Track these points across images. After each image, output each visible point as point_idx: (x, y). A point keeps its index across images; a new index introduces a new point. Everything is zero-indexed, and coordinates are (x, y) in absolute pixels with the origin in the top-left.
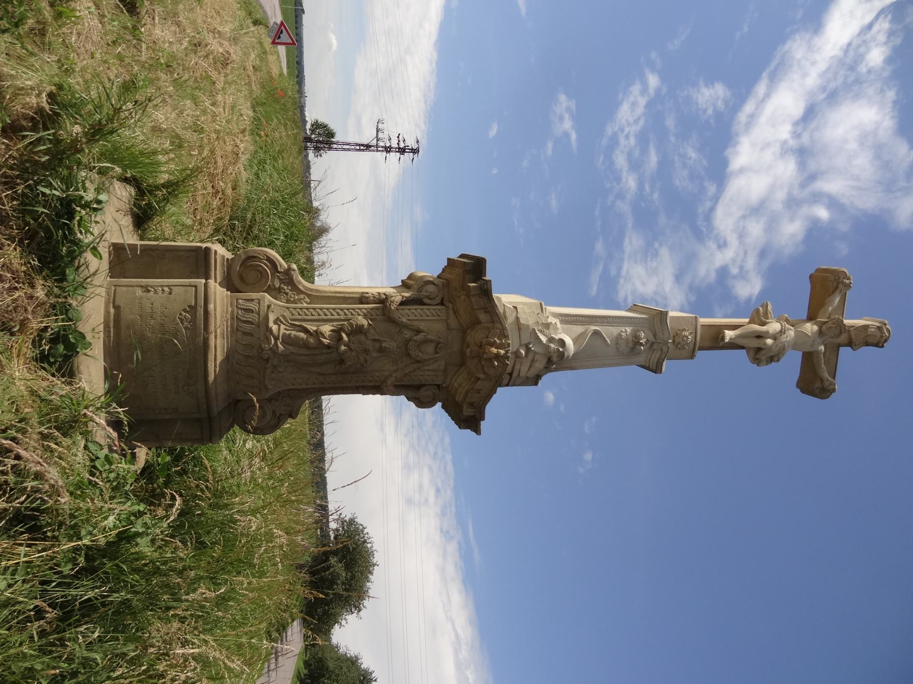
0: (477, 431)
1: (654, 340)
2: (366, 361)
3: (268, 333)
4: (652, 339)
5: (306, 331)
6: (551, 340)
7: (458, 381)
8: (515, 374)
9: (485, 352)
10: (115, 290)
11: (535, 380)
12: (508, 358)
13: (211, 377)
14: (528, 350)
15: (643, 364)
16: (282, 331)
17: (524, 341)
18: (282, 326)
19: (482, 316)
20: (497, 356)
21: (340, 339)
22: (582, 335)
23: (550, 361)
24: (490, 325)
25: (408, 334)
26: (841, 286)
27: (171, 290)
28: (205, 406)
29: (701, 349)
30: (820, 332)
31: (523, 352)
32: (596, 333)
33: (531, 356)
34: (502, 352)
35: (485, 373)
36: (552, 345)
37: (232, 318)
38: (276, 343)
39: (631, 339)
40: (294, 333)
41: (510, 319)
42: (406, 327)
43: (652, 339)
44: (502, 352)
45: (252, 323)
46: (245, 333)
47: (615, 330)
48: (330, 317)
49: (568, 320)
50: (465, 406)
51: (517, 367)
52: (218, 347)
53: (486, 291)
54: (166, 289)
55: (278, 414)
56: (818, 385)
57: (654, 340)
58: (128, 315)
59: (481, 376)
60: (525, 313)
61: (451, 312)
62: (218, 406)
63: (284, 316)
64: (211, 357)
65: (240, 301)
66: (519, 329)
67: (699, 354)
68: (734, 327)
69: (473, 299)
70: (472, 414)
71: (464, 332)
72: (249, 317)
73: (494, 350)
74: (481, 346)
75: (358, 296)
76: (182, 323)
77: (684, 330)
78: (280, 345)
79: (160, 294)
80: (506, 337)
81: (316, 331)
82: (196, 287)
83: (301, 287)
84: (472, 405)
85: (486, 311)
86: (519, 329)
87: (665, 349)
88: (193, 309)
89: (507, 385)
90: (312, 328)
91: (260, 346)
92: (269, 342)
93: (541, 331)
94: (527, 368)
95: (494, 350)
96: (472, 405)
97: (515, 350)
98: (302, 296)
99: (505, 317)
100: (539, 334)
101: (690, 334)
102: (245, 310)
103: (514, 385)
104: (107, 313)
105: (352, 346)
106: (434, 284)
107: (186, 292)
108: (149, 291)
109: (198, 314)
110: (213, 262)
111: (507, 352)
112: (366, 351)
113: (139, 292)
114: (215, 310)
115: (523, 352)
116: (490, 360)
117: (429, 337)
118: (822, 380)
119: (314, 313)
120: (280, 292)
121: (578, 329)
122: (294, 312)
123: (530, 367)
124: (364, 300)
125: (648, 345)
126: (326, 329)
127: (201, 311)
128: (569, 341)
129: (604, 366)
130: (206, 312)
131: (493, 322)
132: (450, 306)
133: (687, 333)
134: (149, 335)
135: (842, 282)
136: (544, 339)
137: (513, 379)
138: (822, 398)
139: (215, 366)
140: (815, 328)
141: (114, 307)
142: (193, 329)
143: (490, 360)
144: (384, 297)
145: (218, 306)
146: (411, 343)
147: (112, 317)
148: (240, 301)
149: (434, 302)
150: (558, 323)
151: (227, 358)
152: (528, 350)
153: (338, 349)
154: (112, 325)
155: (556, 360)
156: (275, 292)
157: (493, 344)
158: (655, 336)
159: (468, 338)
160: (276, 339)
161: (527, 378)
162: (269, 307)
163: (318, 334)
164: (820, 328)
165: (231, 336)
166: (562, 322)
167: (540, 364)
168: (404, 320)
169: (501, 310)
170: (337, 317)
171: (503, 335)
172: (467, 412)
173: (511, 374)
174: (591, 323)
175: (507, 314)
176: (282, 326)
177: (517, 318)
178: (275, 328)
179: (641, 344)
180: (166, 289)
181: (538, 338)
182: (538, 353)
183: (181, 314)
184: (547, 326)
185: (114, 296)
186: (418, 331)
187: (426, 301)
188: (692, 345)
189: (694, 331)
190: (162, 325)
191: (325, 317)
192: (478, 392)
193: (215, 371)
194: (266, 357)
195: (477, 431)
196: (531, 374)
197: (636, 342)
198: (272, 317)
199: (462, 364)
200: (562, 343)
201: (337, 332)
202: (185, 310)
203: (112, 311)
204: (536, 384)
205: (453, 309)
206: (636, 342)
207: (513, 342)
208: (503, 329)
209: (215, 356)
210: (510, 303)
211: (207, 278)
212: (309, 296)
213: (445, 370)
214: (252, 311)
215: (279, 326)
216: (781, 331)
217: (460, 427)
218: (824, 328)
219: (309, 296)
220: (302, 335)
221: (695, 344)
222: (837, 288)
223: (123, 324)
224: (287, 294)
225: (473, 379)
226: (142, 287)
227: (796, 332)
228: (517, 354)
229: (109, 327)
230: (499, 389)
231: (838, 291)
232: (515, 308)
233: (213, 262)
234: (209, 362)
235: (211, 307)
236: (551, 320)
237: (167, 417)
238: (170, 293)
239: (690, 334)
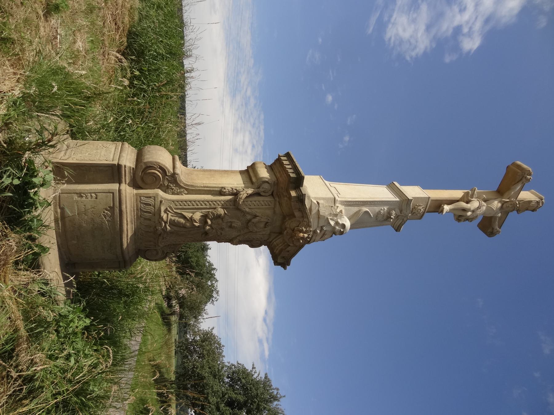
0: (285, 268)
2: (221, 234)
3: (160, 220)
4: (399, 213)
5: (184, 217)
6: (337, 223)
13: (125, 245)
16: (170, 217)
17: (320, 225)
18: (170, 214)
19: (297, 214)
21: (206, 222)
22: (357, 213)
25: (249, 217)
26: (524, 180)
27: (96, 195)
29: (428, 212)
30: (502, 207)
32: (366, 212)
34: (306, 235)
35: (293, 244)
36: (337, 228)
37: (137, 209)
38: (165, 226)
40: (177, 219)
41: (314, 211)
42: (248, 213)
43: (399, 213)
45: (150, 213)
46: (145, 219)
47: (377, 209)
48: (200, 206)
52: (129, 229)
54: (93, 195)
55: (165, 252)
56: (490, 230)
59: (291, 245)
61: (277, 203)
63: (170, 208)
64: (125, 236)
65: (142, 198)
66: (319, 218)
68: (450, 202)
69: (292, 203)
72: (148, 208)
75: (219, 189)
77: (420, 206)
78: (168, 227)
81: (191, 218)
82: (113, 193)
83: (182, 185)
85: (300, 210)
86: (319, 218)
88: (112, 209)
90: (188, 215)
91: (155, 227)
92: (161, 225)
98: (182, 190)
102: (145, 204)
105: (214, 226)
106: (269, 183)
107: (107, 197)
108: (82, 197)
109: (115, 209)
110: (124, 177)
112: (222, 229)
113: (76, 197)
114: (126, 208)
115: (318, 231)
117: (262, 220)
118: (493, 229)
119: (190, 204)
120: (168, 188)
122: (177, 203)
124: (222, 193)
126: (197, 216)
127: (117, 210)
129: (366, 227)
130: (121, 211)
131: (303, 217)
132: (277, 199)
133: (420, 208)
134: (84, 225)
135: (526, 177)
136: (332, 223)
138: (489, 237)
139: (127, 240)
140: (500, 205)
141: (60, 208)
144: (235, 191)
146: (250, 223)
148: (142, 198)
149: (267, 194)
151: (135, 234)
152: (322, 229)
153: (204, 228)
156: (166, 189)
157: (301, 231)
159: (286, 223)
160: (166, 223)
162: (161, 202)
163: (192, 220)
164: (503, 205)
165: (137, 220)
168: (247, 210)
170: (205, 206)
171: (308, 225)
176: (170, 214)
178: (164, 216)
180: (93, 195)
181: (329, 223)
183: (104, 212)
186: (256, 216)
187: (261, 194)
190: (93, 219)
191: (196, 207)
192: (288, 252)
193: (127, 242)
194: (159, 233)
197: (389, 217)
198: (163, 209)
200: (344, 226)
201: (205, 217)
202: (107, 210)
203: (59, 211)
205: (279, 202)
209: (127, 234)
210: (315, 198)
212: (186, 189)
213: (270, 234)
214: (150, 205)
215: (168, 214)
216: (478, 208)
218: (505, 206)
219: (186, 189)
220: (182, 221)
222: (521, 180)
224: (172, 189)
226: (77, 193)
227: (487, 207)
231: (521, 182)
232: (318, 203)
233: (124, 173)
235: (124, 207)
238: (96, 198)
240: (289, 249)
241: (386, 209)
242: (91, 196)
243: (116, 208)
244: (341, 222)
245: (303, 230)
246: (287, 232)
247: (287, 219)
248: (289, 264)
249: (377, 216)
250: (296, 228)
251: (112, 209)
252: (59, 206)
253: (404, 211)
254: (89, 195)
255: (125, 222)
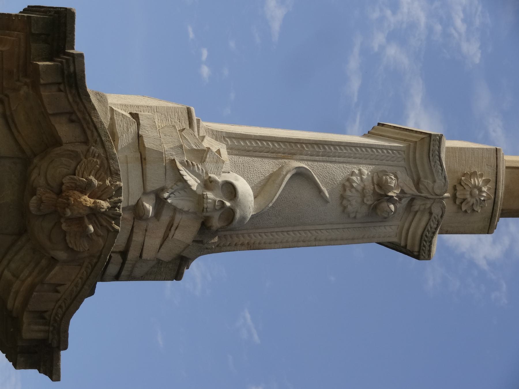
0: (52, 371)
1: (415, 191)
4: (411, 190)
6: (208, 184)
7: (13, 265)
8: (132, 254)
9: (68, 205)
11: (174, 268)
12: (116, 218)
14: (160, 203)
15: (395, 240)
17: (153, 185)
19: (64, 130)
20: (94, 213)
22: (272, 178)
23: (205, 226)
24: (81, 149)
29: (508, 213)
31: (149, 207)
32: (301, 175)
33: (165, 218)
34: (105, 204)
35: (68, 249)
36: (210, 195)
39: (370, 188)
43: (411, 190)
44: (105, 204)
49: (245, 147)
50: (26, 319)
51: (137, 238)
53: (72, 76)
57: (415, 191)
59: (62, 255)
60: (154, 126)
66: (143, 160)
67: (502, 223)
69: (45, 93)
70: (40, 335)
71: (25, 162)
73: (88, 201)
74: (60, 193)
77: (474, 174)
80: (115, 174)
84: (40, 316)
86: (143, 160)
87: (436, 210)
89: (117, 278)
93: (187, 165)
94: (158, 242)
95: (88, 201)
96: (40, 316)
97: (132, 202)
99: (114, 134)
100: (183, 172)
101: (487, 182)
103: (131, 278)
111: (115, 205)
115: (149, 207)
116: (79, 221)
121: (266, 166)
123: (165, 238)
125: (405, 201)
128: (244, 186)
129: (317, 242)
131: (86, 142)
133: (479, 181)
136: (193, 182)
137: (128, 266)
143: (79, 221)
150: (224, 152)
152: (160, 203)
155: (217, 228)
157: (85, 188)
158: (417, 183)
159: (34, 175)
161: (159, 262)
166: (231, 150)
167: (185, 234)
169: (105, 119)
172: (31, 331)
173: (124, 254)
174: (291, 155)
175: (118, 129)
177: (139, 137)
179: (390, 199)
181: (181, 179)
182: (181, 211)
184: (202, 154)
188: (488, 205)
189: (493, 179)
192: (55, 288)
195: (52, 371)
196: (167, 254)
199: (22, 231)
200: (230, 190)
204: (178, 276)
206: (380, 194)
207: (130, 188)
208: (109, 157)
210: (125, 106)
217: (15, 366)
221: (495, 203)
225: (44, 262)
228: (137, 211)
230: (100, 285)
232: (135, 116)
236: (209, 143)
239: (487, 182)
240: (56, 274)
241: (366, 172)
244: (220, 179)
245: (90, 182)
246: (41, 201)
247: (35, 161)
248: (62, 343)
249: (342, 197)
250: (66, 180)
253: (427, 182)
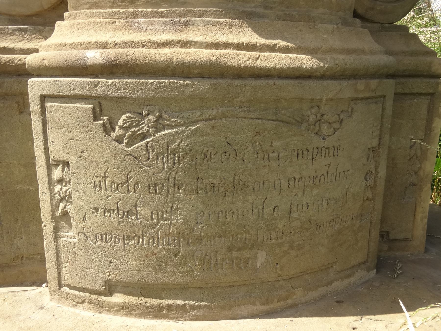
10: (69, 286)
13: (305, 61)
27: (57, 163)
28: (374, 83)
54: (57, 173)
58: (129, 263)
62: (366, 49)
64: (243, 59)
76: (144, 136)
79: (70, 188)
82: (44, 98)
88: (101, 108)
104: (122, 309)
107: (58, 124)
108: (65, 214)
113: (69, 236)
114: (105, 46)
127: (107, 85)
130: (110, 69)
134: (178, 220)
139: (272, 49)
141: (110, 293)
142: (161, 108)
145: (93, 39)
147: (133, 300)
151: (251, 18)
154: (155, 302)
180: (57, 173)
183: (119, 140)
185: (83, 290)
190: (152, 187)
193: (286, 50)
202: (108, 129)
203: (118, 298)
209: (241, 47)
211: (23, 73)
223: (150, 277)
226: (56, 229)
229: (160, 308)
234: (260, 63)
235: (94, 56)
237: (382, 173)
238: (66, 164)
242: (60, 181)
243: (99, 90)
251: (135, 105)
252: (100, 294)
254: (58, 187)
255: (165, 53)
